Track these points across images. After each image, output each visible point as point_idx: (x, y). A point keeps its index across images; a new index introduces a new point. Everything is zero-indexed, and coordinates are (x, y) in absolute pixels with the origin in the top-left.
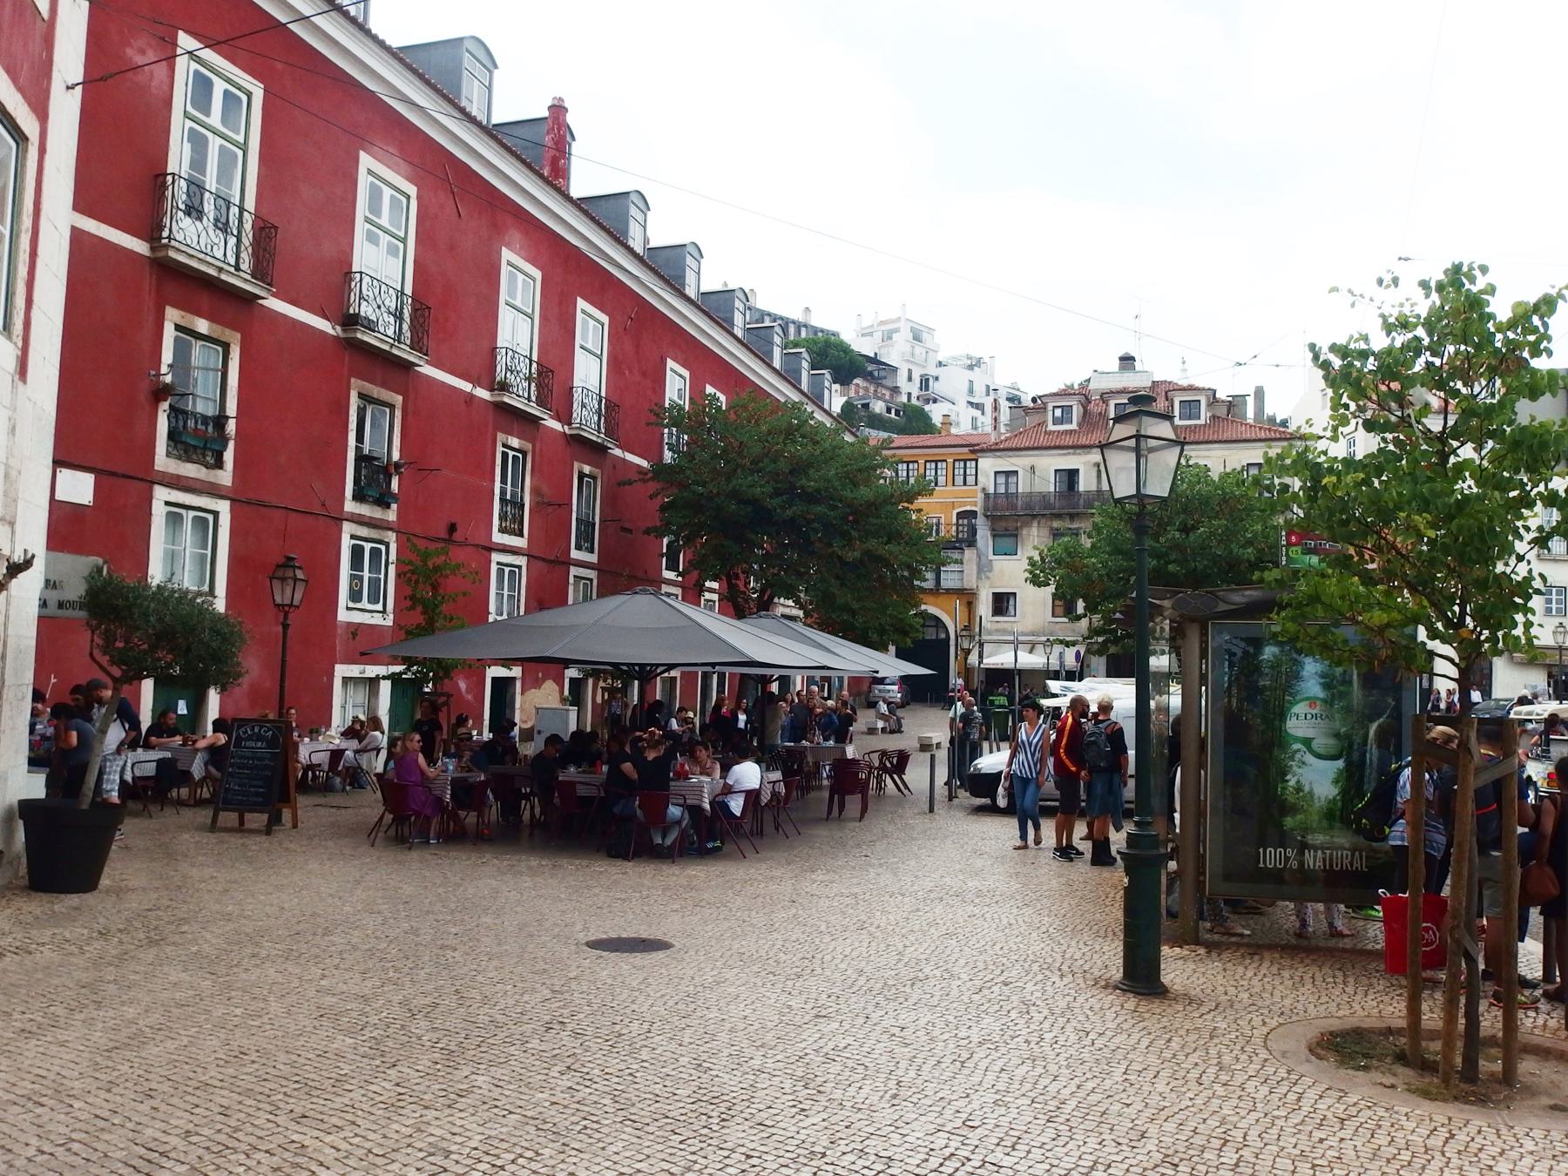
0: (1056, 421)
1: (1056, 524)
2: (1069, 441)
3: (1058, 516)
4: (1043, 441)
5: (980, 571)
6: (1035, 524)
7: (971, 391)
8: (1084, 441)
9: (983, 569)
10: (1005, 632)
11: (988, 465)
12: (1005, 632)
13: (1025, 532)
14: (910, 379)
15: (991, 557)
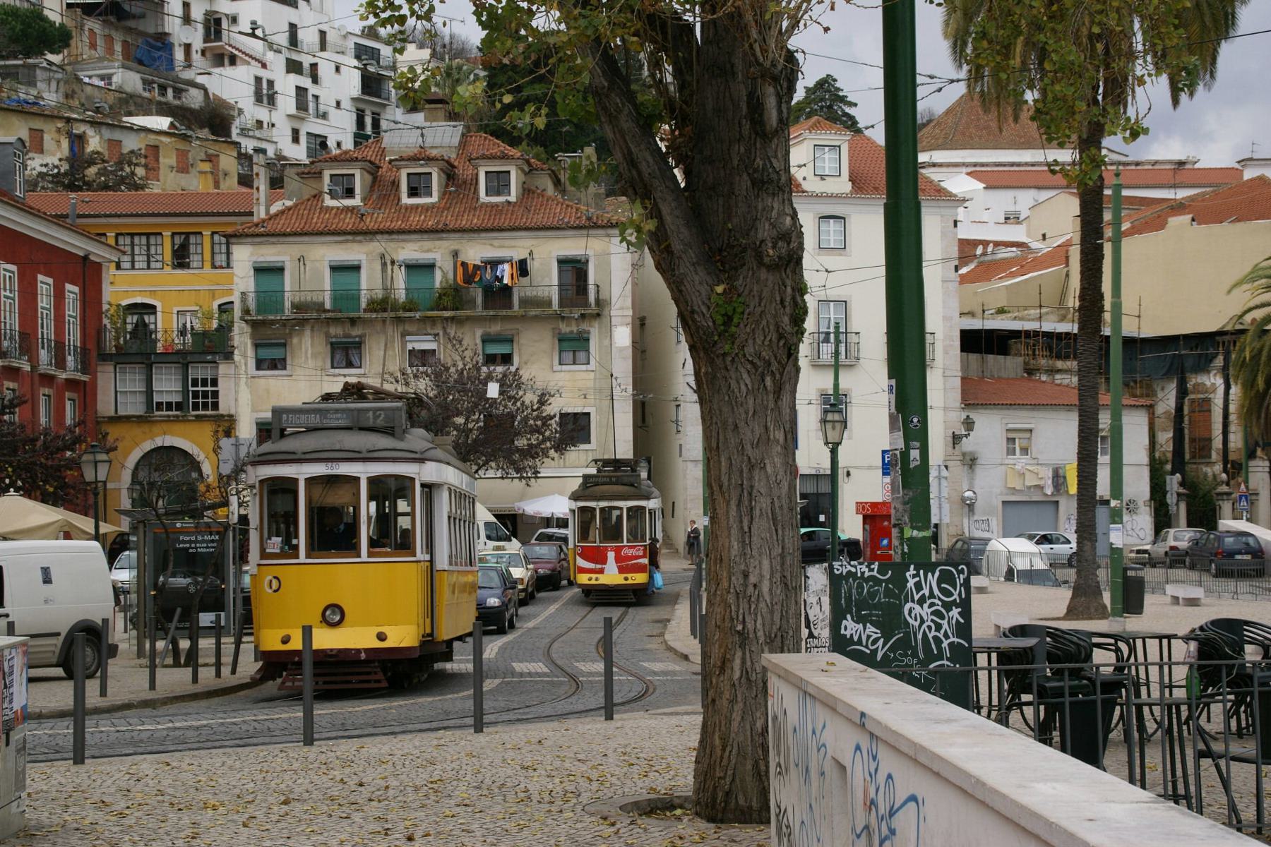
1: (336, 331)
2: (349, 222)
3: (336, 321)
4: (317, 221)
6: (308, 332)
7: (294, 41)
8: (369, 223)
11: (244, 256)
13: (295, 340)
14: (187, 19)
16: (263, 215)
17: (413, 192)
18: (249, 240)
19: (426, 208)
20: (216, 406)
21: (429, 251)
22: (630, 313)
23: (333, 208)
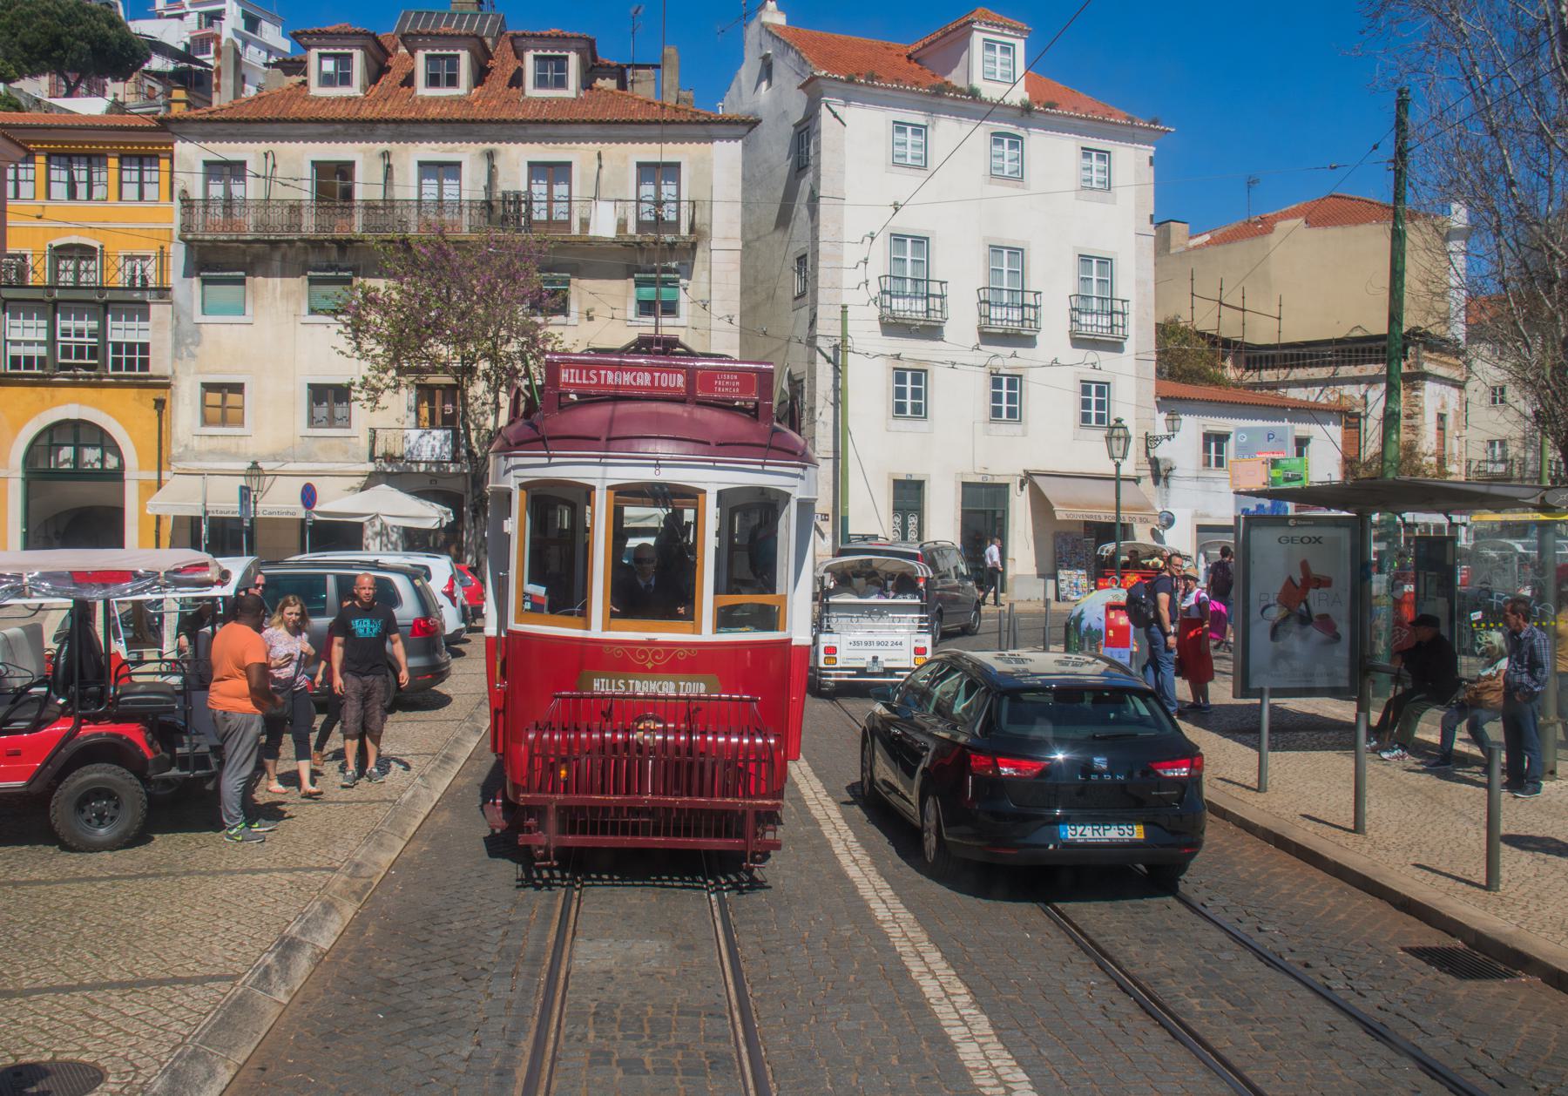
0: (327, 80)
2: (341, 112)
4: (296, 110)
5: (178, 343)
8: (367, 113)
9: (185, 339)
10: (225, 454)
12: (225, 454)
15: (199, 318)
16: (225, 104)
17: (433, 81)
18: (197, 127)
19: (450, 101)
20: (145, 364)
21: (451, 151)
22: (739, 245)
23: (320, 99)
